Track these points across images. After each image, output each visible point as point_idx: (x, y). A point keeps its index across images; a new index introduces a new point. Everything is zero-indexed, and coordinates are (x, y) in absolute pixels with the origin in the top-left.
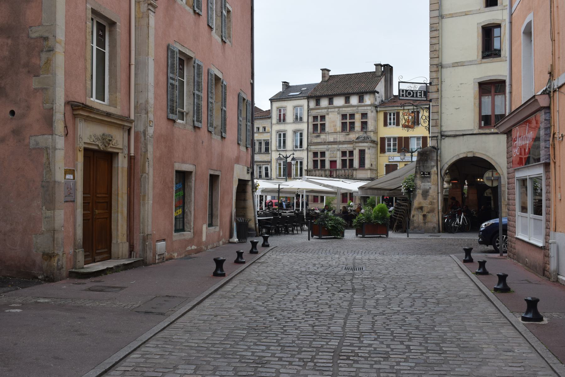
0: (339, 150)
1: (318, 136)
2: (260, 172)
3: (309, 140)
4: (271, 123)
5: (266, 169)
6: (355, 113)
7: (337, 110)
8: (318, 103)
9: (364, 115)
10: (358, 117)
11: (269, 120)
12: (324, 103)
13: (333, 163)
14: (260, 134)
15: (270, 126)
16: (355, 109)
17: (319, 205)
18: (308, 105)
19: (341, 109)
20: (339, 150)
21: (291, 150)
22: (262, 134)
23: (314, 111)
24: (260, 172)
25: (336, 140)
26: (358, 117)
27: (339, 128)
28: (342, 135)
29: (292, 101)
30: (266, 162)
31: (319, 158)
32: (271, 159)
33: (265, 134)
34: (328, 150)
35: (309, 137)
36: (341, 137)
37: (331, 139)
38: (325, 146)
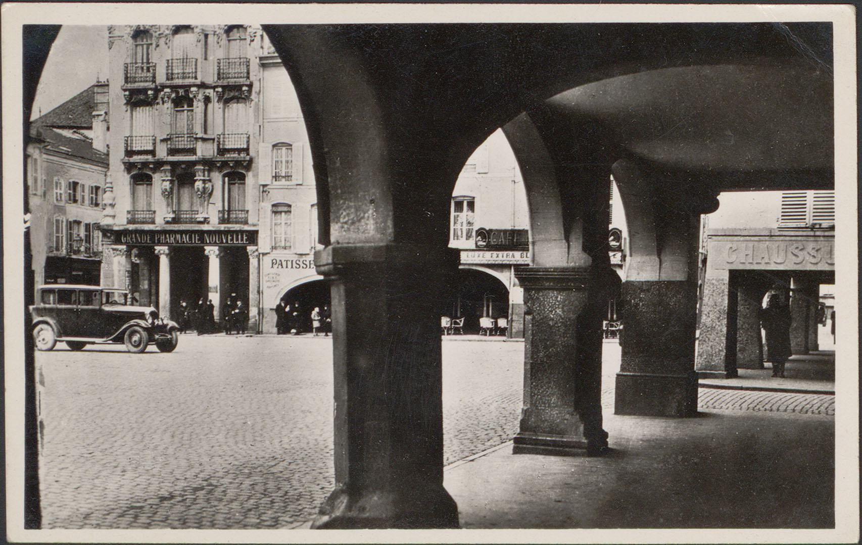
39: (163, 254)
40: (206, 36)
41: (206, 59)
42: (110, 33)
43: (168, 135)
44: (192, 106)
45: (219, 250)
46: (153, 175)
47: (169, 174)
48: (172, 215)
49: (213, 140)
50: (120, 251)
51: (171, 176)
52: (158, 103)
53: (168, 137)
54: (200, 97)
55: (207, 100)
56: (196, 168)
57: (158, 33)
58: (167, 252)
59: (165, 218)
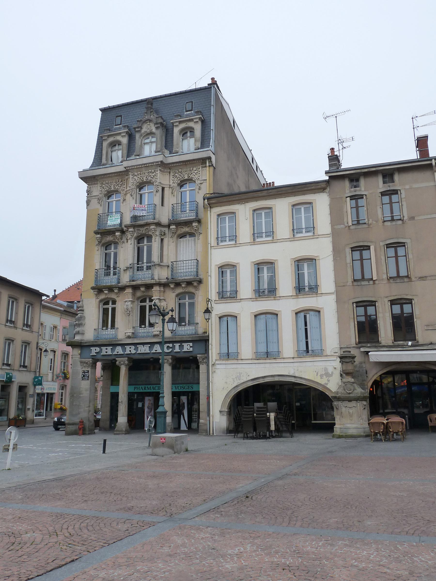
39: (123, 364)
40: (163, 189)
41: (162, 205)
42: (88, 194)
43: (130, 264)
45: (171, 359)
46: (117, 299)
48: (131, 331)
49: (168, 266)
50: (87, 363)
51: (132, 298)
52: (123, 242)
53: (131, 266)
54: (158, 233)
56: (152, 290)
57: (125, 191)
58: (126, 362)
59: (125, 333)
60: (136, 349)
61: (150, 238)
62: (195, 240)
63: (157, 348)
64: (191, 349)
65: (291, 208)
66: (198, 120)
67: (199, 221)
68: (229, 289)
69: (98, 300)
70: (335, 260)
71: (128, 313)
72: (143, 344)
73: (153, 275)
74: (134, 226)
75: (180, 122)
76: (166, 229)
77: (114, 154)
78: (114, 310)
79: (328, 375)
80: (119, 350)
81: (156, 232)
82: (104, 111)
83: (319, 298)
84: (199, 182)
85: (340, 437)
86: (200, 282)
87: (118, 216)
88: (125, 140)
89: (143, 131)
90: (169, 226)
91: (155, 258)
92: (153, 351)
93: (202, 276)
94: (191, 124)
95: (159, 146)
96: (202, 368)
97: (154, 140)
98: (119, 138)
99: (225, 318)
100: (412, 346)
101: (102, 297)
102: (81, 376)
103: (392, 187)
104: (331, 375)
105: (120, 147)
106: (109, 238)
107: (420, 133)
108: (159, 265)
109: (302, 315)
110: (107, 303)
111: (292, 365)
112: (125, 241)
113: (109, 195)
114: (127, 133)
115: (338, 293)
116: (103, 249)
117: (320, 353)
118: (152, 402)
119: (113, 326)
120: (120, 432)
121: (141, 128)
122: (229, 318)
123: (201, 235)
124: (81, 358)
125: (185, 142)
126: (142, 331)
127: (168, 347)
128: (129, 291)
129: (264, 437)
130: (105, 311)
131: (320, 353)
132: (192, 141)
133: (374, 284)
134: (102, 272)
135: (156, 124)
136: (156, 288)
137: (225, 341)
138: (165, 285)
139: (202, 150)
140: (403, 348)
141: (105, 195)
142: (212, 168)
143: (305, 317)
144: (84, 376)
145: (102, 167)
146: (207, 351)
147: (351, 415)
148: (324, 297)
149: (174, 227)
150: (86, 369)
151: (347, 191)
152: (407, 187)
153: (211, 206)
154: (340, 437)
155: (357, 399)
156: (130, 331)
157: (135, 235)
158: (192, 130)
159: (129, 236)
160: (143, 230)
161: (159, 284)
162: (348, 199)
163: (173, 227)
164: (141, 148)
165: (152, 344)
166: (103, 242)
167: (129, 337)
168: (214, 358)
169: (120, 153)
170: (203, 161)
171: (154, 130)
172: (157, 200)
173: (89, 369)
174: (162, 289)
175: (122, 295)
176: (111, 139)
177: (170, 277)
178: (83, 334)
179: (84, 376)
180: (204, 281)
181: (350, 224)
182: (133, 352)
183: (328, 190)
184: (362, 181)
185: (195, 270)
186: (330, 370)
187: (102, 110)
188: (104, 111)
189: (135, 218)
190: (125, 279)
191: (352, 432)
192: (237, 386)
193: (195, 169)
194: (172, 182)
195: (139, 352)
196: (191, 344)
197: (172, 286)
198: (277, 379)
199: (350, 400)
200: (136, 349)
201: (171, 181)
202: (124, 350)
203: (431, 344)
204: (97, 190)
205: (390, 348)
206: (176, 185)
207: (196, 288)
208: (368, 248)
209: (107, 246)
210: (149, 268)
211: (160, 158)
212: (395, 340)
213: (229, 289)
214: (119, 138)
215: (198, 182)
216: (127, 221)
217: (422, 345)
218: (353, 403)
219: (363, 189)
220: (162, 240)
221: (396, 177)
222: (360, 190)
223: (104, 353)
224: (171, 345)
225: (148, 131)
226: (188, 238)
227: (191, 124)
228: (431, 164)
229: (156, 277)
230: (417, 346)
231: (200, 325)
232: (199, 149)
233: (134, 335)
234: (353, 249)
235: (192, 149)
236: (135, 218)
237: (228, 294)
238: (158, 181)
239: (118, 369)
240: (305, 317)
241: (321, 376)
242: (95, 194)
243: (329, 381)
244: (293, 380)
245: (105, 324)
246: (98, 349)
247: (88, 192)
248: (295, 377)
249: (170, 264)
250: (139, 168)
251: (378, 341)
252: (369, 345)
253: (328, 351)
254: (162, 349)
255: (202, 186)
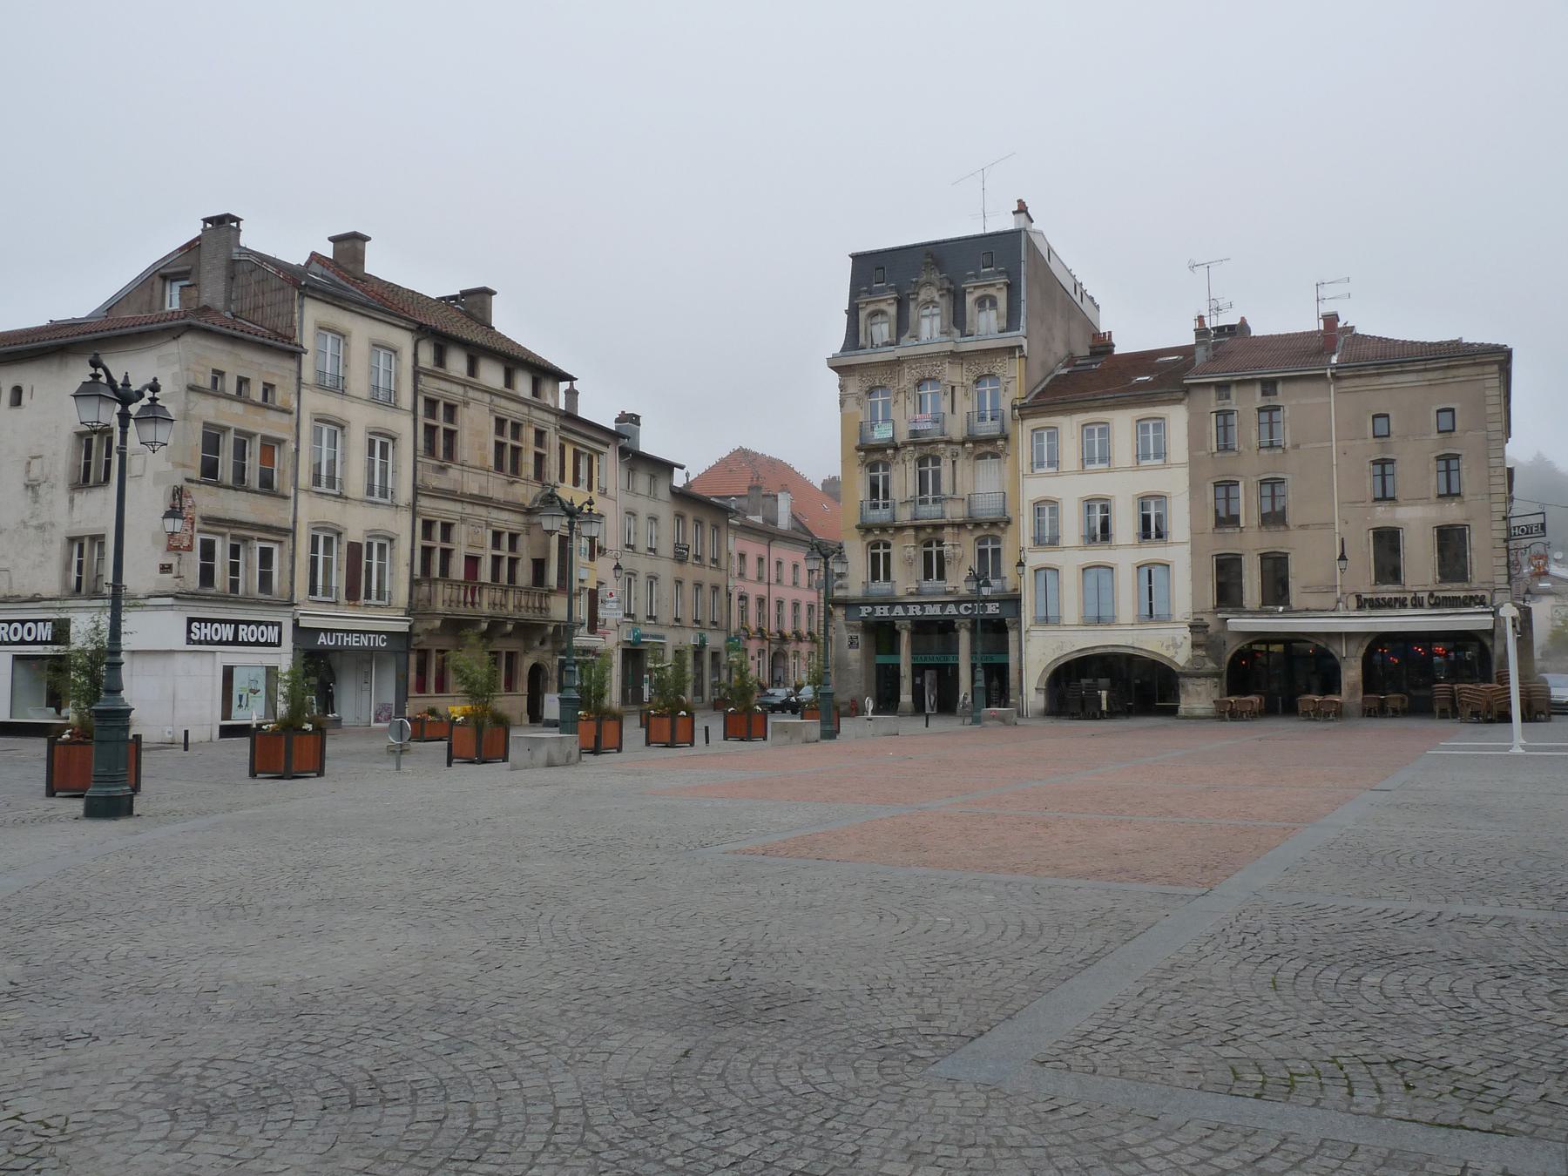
0: (488, 525)
1: (443, 469)
2: (234, 569)
3: (419, 477)
4: (299, 378)
5: (266, 555)
6: (525, 424)
7: (487, 398)
8: (440, 360)
9: (540, 435)
10: (529, 434)
11: (291, 365)
12: (457, 363)
13: (472, 562)
14: (251, 409)
15: (294, 388)
16: (525, 410)
17: (435, 700)
18: (415, 355)
19: (497, 400)
20: (488, 525)
21: (362, 501)
22: (261, 410)
23: (430, 379)
24: (234, 569)
25: (484, 494)
26: (529, 434)
27: (491, 461)
28: (499, 481)
29: (367, 320)
30: (267, 528)
31: (437, 542)
32: (295, 522)
33: (273, 417)
34: (463, 520)
35: (419, 466)
36: (496, 487)
37: (473, 485)
38: (457, 507)
40: (953, 388)
44: (939, 464)
47: (913, 540)
52: (898, 463)
55: (955, 455)
58: (909, 626)
60: (923, 610)
61: (937, 461)
62: (999, 463)
63: (951, 610)
64: (998, 611)
65: (1135, 424)
66: (1002, 286)
67: (1006, 438)
68: (1047, 534)
69: (865, 543)
70: (1191, 498)
71: (909, 562)
72: (932, 603)
73: (943, 512)
74: (915, 444)
75: (975, 287)
76: (959, 448)
77: (875, 329)
78: (887, 556)
79: (1176, 646)
80: (899, 611)
81: (945, 452)
82: (858, 259)
83: (1169, 549)
84: (1005, 380)
85: (1185, 718)
86: (1008, 522)
87: (890, 426)
88: (892, 310)
89: (921, 298)
90: (963, 443)
91: (946, 489)
92: (946, 613)
93: (1009, 514)
94: (991, 291)
95: (945, 323)
96: (1012, 635)
97: (936, 311)
98: (883, 306)
99: (1043, 572)
100: (1284, 611)
101: (871, 538)
102: (847, 642)
103: (1273, 401)
104: (1180, 647)
105: (885, 319)
106: (877, 456)
107: (1327, 308)
108: (951, 498)
109: (1145, 570)
110: (875, 545)
111: (1130, 632)
112: (901, 462)
113: (871, 391)
114: (895, 299)
115: (1193, 543)
116: (867, 470)
117: (1167, 619)
118: (935, 676)
119: (887, 577)
120: (904, 714)
121: (918, 294)
122: (1048, 572)
123: (1009, 458)
124: (846, 620)
125: (983, 315)
126: (928, 586)
127: (966, 608)
128: (911, 532)
129: (1094, 717)
130: (875, 557)
131: (1167, 619)
132: (993, 314)
133: (1241, 531)
134: (867, 504)
135: (941, 289)
136: (948, 530)
137: (1042, 600)
138: (960, 526)
139: (1008, 334)
140: (1271, 614)
141: (867, 392)
142: (1023, 360)
143: (1150, 572)
144: (852, 645)
145: (861, 352)
146: (1018, 613)
147: (1199, 694)
148: (1177, 548)
149: (971, 445)
150: (854, 634)
151: (1213, 404)
152: (1294, 402)
153: (1023, 417)
154: (1185, 718)
155: (1207, 676)
156: (913, 587)
157: (916, 455)
158: (994, 304)
159: (907, 457)
160: (927, 450)
161: (953, 525)
162: (1214, 415)
163: (969, 445)
164: (918, 323)
165: (945, 604)
166: (868, 461)
167: (912, 594)
168: (1028, 623)
169: (885, 328)
170: (1011, 351)
171: (937, 298)
172: (945, 406)
173: (859, 635)
174: (956, 529)
175: (899, 537)
176: (871, 308)
177: (966, 514)
178: (847, 588)
179: (852, 645)
180: (1014, 520)
181: (1215, 450)
182: (919, 613)
183: (1187, 400)
184: (1234, 392)
185: (1001, 506)
186: (1179, 640)
187: (851, 256)
188: (858, 259)
189: (914, 433)
190: (904, 515)
191: (1198, 712)
192: (1058, 659)
193: (998, 360)
194: (965, 378)
195: (927, 613)
196: (997, 605)
197: (970, 527)
198: (1110, 650)
199: (1198, 676)
200: (923, 610)
201: (965, 378)
202: (906, 610)
203: (1307, 610)
204: (855, 385)
205: (1254, 613)
206: (971, 382)
207: (1003, 530)
208: (1236, 484)
209: (873, 467)
210: (935, 501)
211: (949, 347)
212: (1263, 604)
213: (1047, 534)
214: (883, 306)
215: (1003, 380)
216: (903, 437)
217: (1296, 611)
218: (1202, 681)
219: (1234, 403)
220: (954, 462)
221: (1280, 388)
222: (1230, 404)
223: (878, 614)
224: (970, 606)
225: (929, 299)
226: (989, 459)
227: (991, 291)
228: (1326, 374)
229: (948, 516)
230: (1290, 612)
231: (1008, 580)
232: (1003, 331)
233: (919, 592)
234: (1216, 485)
235: (994, 327)
236: (914, 433)
237: (1047, 540)
238: (947, 378)
239: (898, 633)
240: (1150, 572)
241: (1168, 648)
242: (851, 390)
243: (1176, 653)
244: (1131, 651)
245: (875, 577)
246: (870, 609)
247: (842, 387)
248: (1133, 648)
249: (966, 499)
250: (918, 358)
251: (1241, 605)
252: (1230, 609)
253: (1178, 617)
254: (958, 610)
255: (1009, 386)
